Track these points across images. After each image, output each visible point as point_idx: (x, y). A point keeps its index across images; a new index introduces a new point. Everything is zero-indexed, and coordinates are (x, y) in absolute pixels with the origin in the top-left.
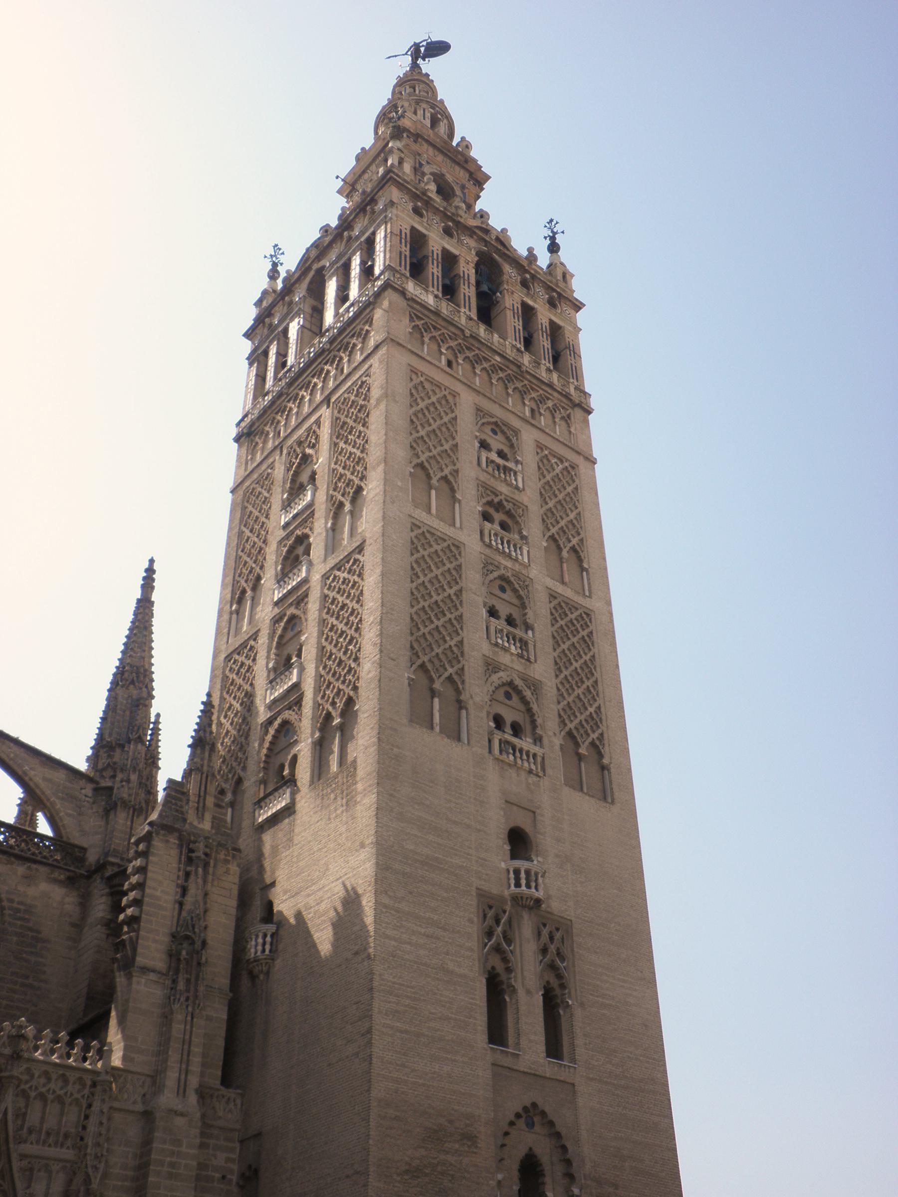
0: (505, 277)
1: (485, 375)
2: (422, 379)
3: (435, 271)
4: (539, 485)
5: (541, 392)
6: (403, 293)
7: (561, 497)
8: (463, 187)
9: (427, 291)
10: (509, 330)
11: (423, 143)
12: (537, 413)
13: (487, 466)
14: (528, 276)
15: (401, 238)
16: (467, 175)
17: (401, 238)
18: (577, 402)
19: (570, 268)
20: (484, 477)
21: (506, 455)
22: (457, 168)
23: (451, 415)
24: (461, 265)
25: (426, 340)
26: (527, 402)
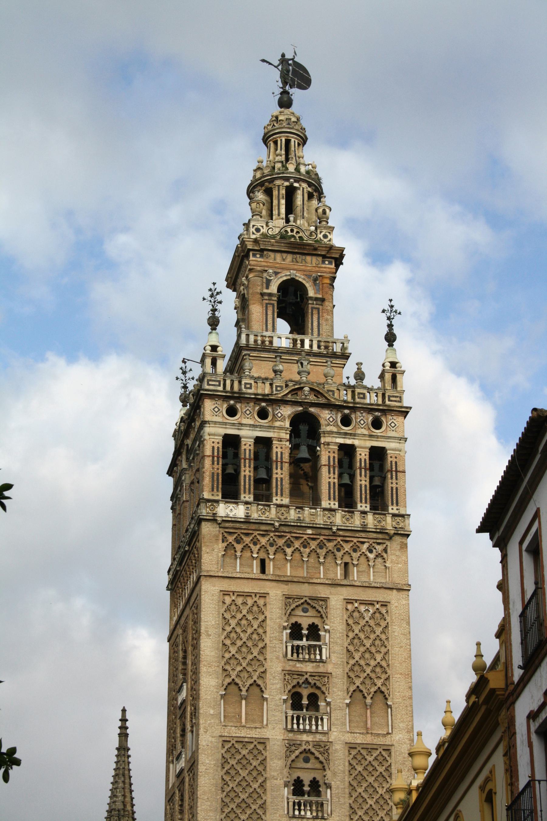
0: (323, 428)
1: (297, 555)
2: (233, 598)
3: (247, 473)
4: (346, 644)
5: (355, 540)
6: (213, 520)
7: (368, 643)
8: (315, 280)
9: (237, 503)
10: (323, 491)
11: (270, 253)
12: (351, 566)
13: (292, 656)
14: (347, 411)
15: (213, 457)
16: (320, 259)
17: (213, 457)
18: (392, 532)
19: (403, 365)
20: (289, 666)
21: (317, 626)
22: (308, 258)
23: (261, 618)
24: (274, 447)
25: (238, 554)
26: (339, 562)
